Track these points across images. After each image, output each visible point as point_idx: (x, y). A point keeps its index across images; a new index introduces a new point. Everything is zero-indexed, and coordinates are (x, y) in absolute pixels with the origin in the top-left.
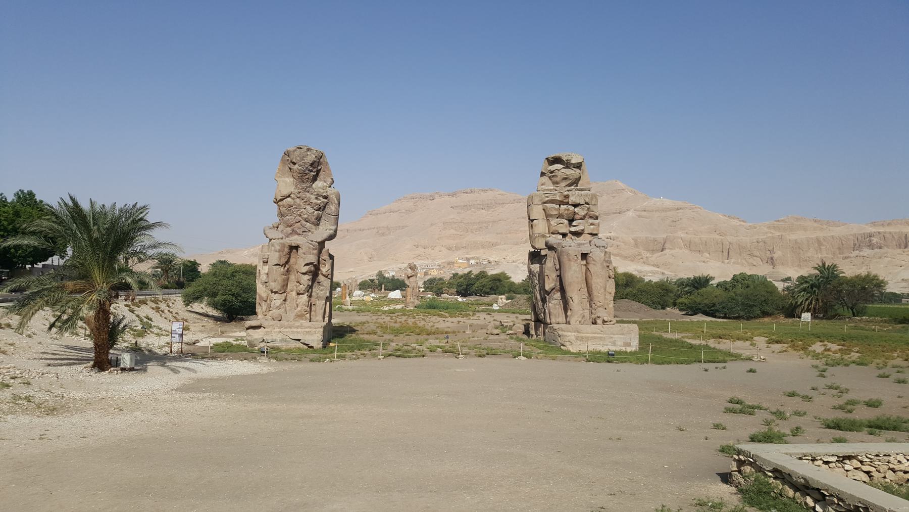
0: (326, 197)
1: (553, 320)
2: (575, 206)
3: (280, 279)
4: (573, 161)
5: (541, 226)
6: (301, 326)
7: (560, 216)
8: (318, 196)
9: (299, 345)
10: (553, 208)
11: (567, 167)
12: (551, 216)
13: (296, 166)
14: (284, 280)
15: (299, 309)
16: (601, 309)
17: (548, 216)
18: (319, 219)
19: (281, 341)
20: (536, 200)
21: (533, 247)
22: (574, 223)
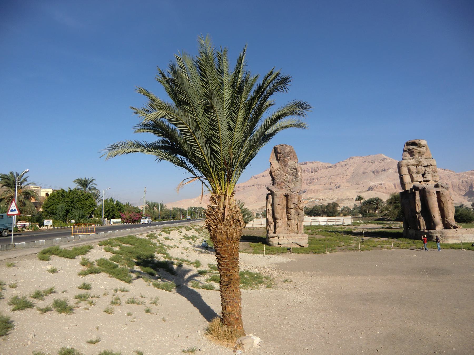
0: (296, 169)
1: (422, 228)
3: (280, 212)
4: (422, 144)
11: (419, 147)
12: (413, 172)
14: (282, 213)
19: (287, 244)
22: (425, 176)
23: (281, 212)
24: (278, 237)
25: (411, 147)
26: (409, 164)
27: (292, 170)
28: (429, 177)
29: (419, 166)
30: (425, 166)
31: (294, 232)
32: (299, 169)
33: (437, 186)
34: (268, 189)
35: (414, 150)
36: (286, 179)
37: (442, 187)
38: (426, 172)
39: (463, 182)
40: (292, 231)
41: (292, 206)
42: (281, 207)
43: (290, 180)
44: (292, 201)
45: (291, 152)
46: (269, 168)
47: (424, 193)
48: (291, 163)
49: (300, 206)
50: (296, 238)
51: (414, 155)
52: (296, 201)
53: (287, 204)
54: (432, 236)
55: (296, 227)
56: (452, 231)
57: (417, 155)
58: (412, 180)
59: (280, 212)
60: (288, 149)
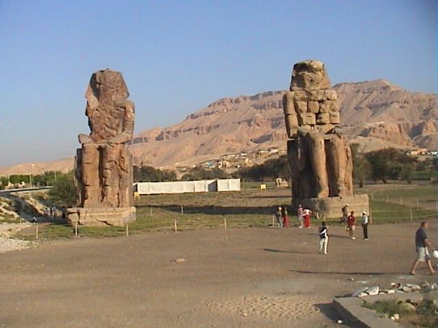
2: (321, 102)
4: (315, 67)
5: (294, 120)
12: (301, 111)
13: (101, 86)
15: (105, 198)
18: (118, 125)
19: (91, 223)
21: (289, 137)
22: (320, 116)
24: (79, 213)
26: (297, 97)
27: (118, 110)
28: (325, 118)
29: (311, 100)
30: (319, 102)
31: (112, 206)
33: (330, 132)
37: (335, 133)
38: (322, 110)
41: (108, 165)
43: (114, 126)
44: (107, 158)
49: (122, 165)
50: (105, 214)
51: (305, 84)
55: (116, 197)
57: (308, 84)
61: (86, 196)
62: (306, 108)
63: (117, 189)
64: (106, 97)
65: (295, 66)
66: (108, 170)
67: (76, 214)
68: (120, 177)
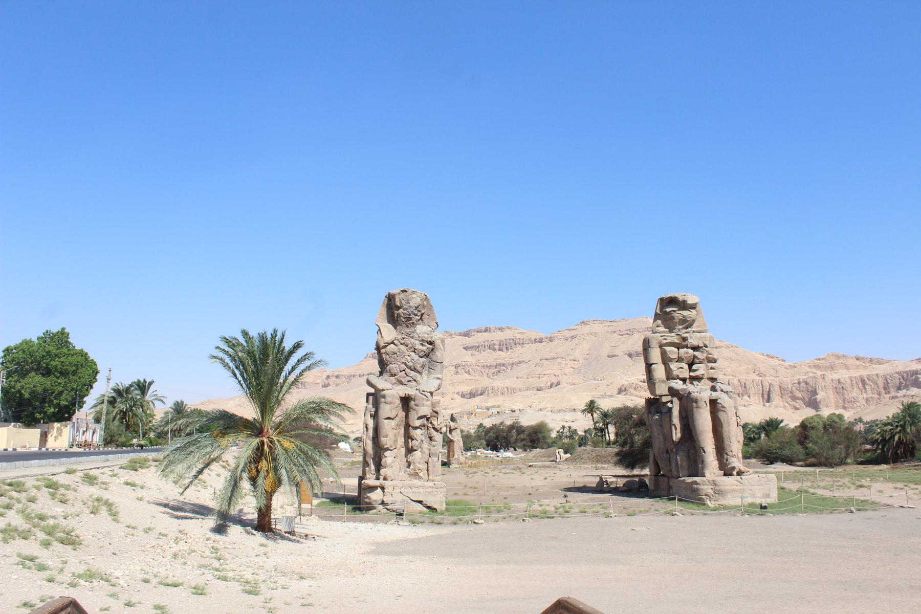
0: (431, 343)
2: (695, 348)
4: (690, 302)
5: (659, 371)
6: (423, 487)
7: (680, 360)
8: (422, 342)
9: (420, 507)
10: (672, 351)
12: (671, 360)
13: (401, 310)
15: (412, 467)
16: (734, 459)
17: (666, 360)
20: (654, 343)
22: (694, 367)
23: (392, 433)
24: (383, 488)
25: (670, 309)
29: (683, 348)
31: (420, 478)
32: (438, 343)
34: (369, 383)
35: (675, 315)
36: (410, 364)
39: (799, 383)
40: (416, 475)
42: (393, 423)
43: (419, 368)
45: (424, 307)
46: (375, 338)
47: (687, 403)
48: (422, 330)
49: (435, 423)
50: (421, 490)
52: (425, 410)
53: (407, 416)
54: (698, 489)
56: (732, 480)
58: (670, 376)
59: (391, 434)
60: (416, 301)
61: (383, 463)
62: (676, 356)
63: (426, 457)
64: (407, 326)
65: (661, 300)
66: (419, 430)
67: (379, 490)
68: (431, 438)
